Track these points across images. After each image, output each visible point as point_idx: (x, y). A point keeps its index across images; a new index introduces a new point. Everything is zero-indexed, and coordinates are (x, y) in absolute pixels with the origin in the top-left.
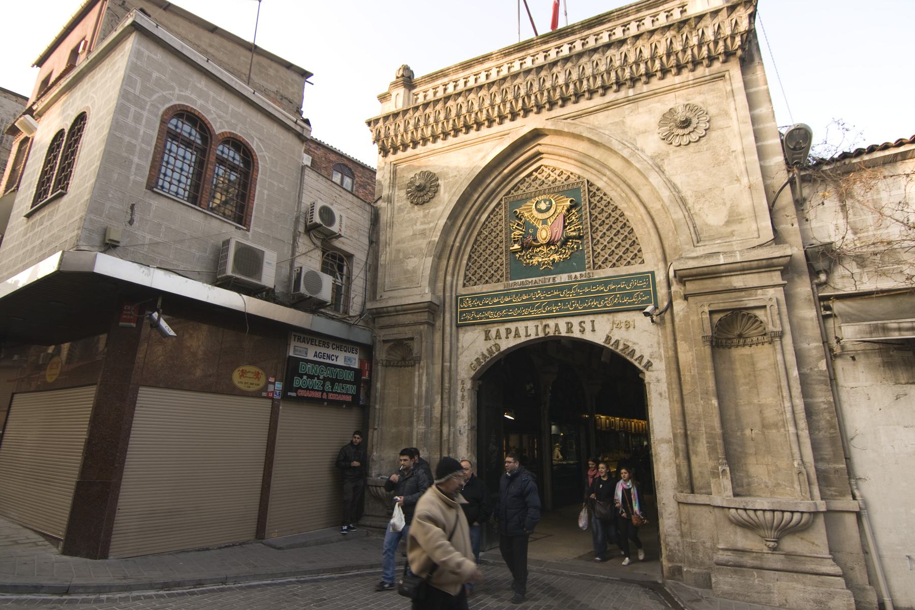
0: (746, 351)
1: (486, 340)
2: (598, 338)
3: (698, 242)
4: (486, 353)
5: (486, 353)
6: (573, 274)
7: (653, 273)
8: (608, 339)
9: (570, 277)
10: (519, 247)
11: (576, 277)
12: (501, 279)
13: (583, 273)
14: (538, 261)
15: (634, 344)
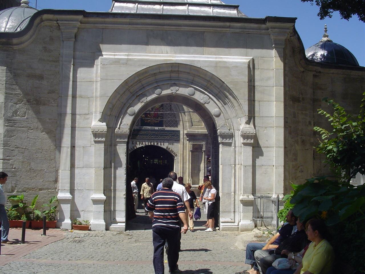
0: (197, 153)
1: (132, 144)
2: (165, 147)
3: (192, 126)
4: (132, 148)
5: (132, 148)
6: (160, 127)
7: (180, 131)
8: (167, 147)
9: (159, 128)
10: (144, 116)
11: (160, 128)
12: (138, 125)
13: (162, 127)
14: (150, 122)
15: (174, 149)
